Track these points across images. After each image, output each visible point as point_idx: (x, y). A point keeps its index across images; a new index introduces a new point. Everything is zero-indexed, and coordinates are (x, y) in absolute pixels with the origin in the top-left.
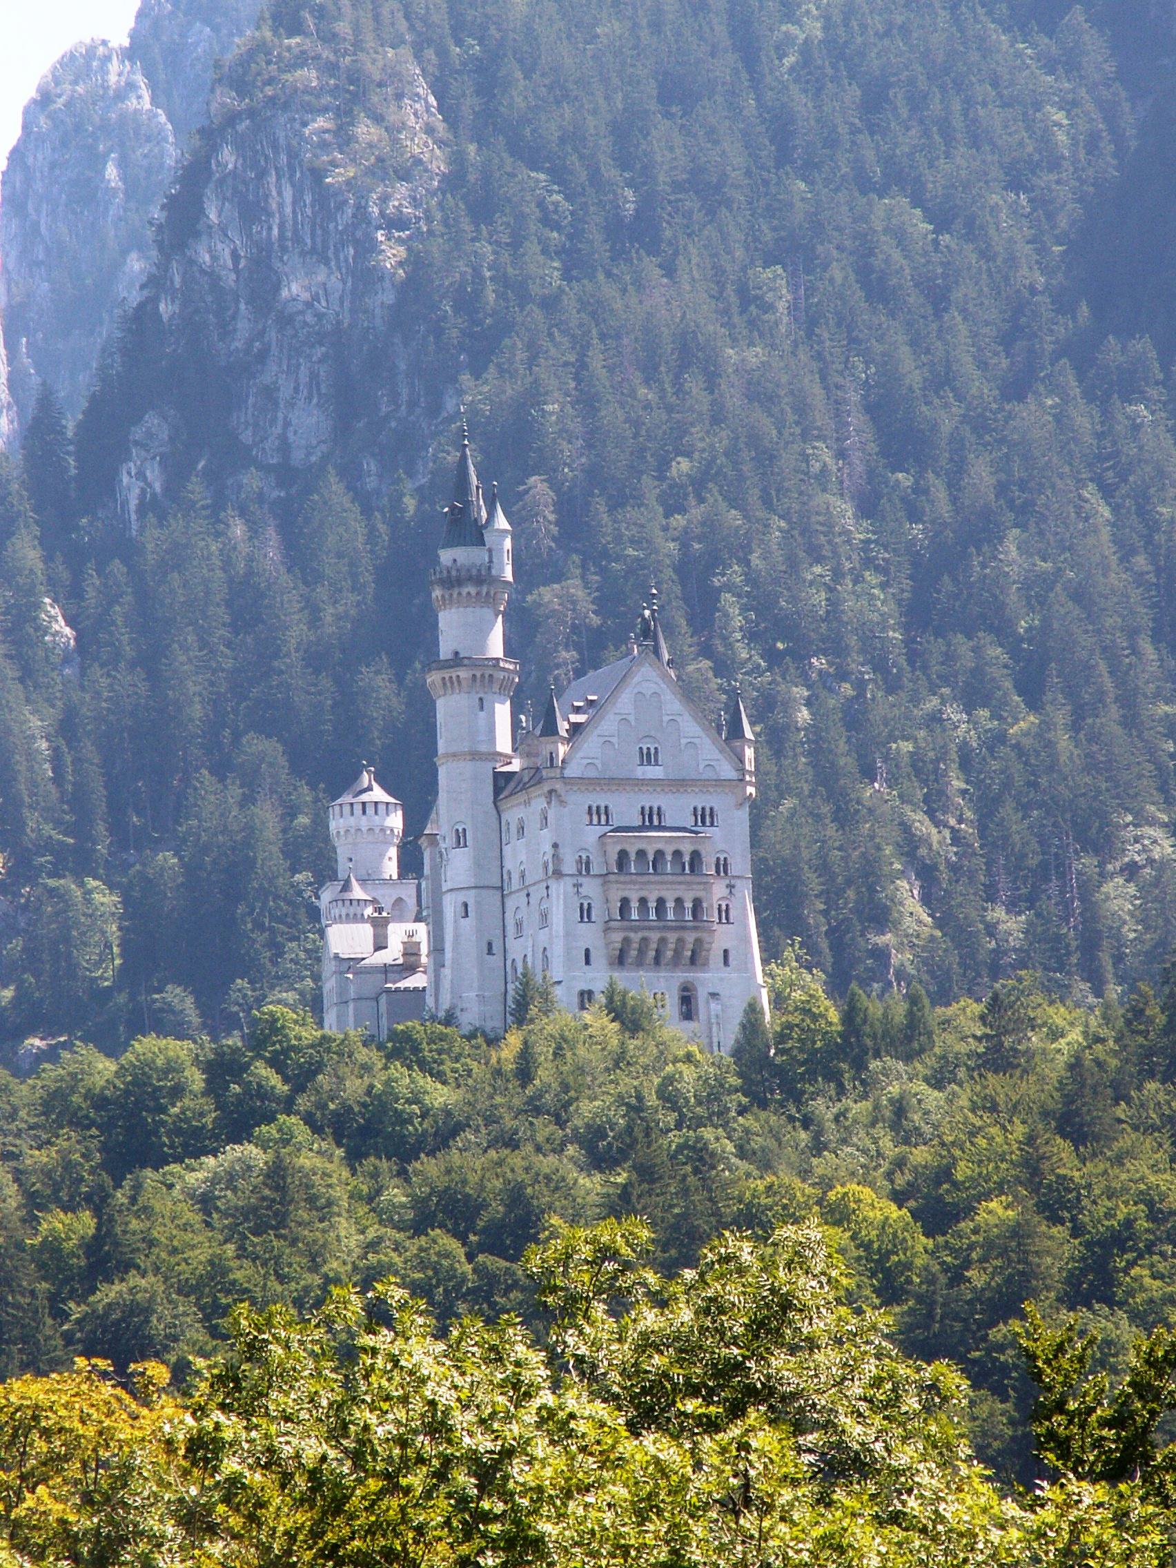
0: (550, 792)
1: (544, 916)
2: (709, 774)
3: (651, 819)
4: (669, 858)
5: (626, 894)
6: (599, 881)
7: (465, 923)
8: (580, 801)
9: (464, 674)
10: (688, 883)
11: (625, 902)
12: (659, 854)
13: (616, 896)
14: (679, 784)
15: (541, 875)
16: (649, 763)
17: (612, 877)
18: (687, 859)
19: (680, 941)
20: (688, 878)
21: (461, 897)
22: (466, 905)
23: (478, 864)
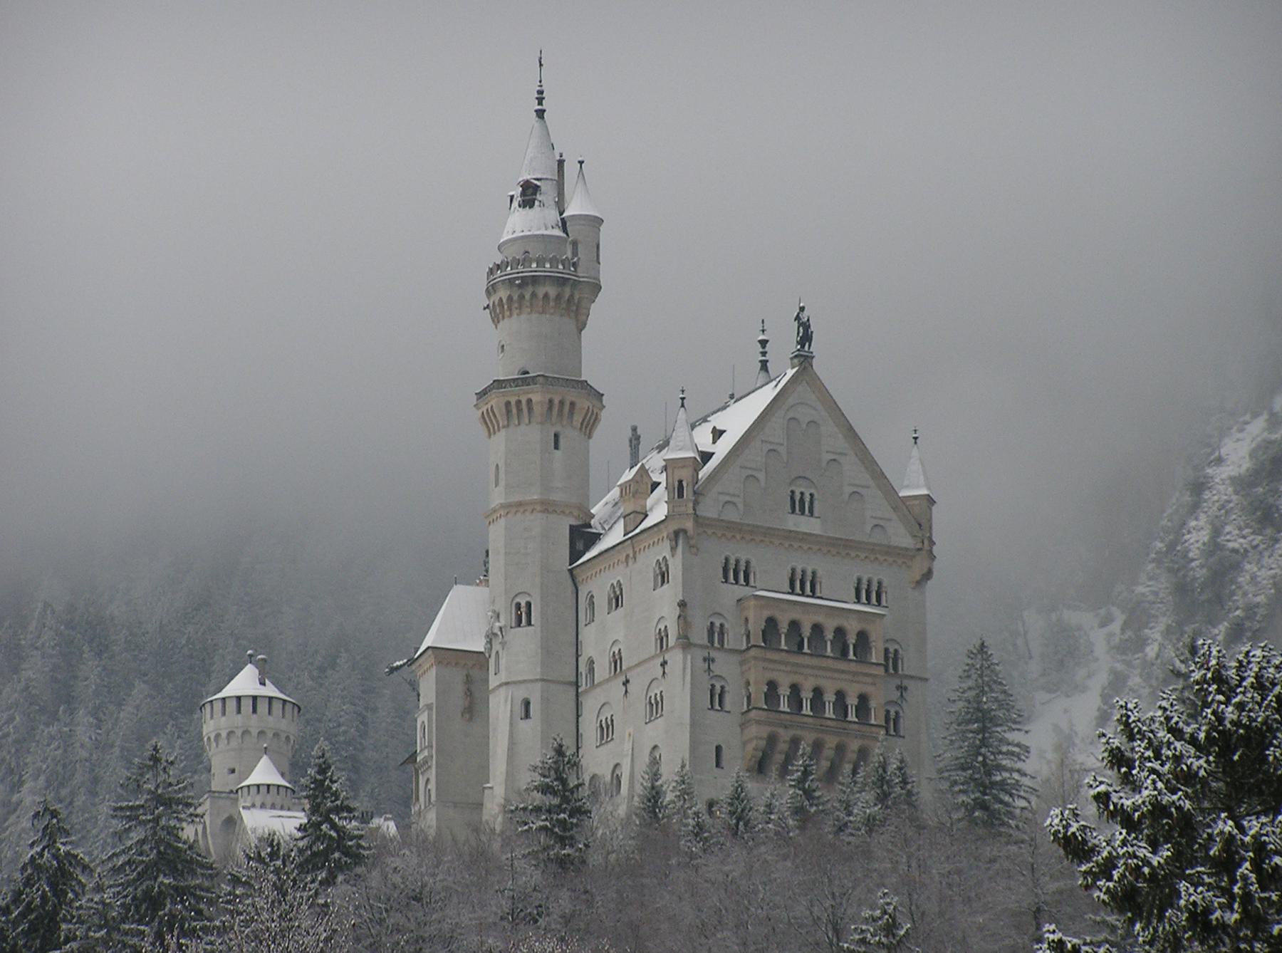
0: (677, 533)
1: (655, 706)
4: (829, 635)
6: (735, 658)
7: (524, 725)
10: (855, 674)
11: (772, 685)
13: (758, 677)
14: (840, 547)
15: (651, 647)
16: (803, 513)
17: (753, 652)
18: (852, 640)
20: (853, 667)
21: (521, 693)
22: (527, 704)
23: (547, 651)
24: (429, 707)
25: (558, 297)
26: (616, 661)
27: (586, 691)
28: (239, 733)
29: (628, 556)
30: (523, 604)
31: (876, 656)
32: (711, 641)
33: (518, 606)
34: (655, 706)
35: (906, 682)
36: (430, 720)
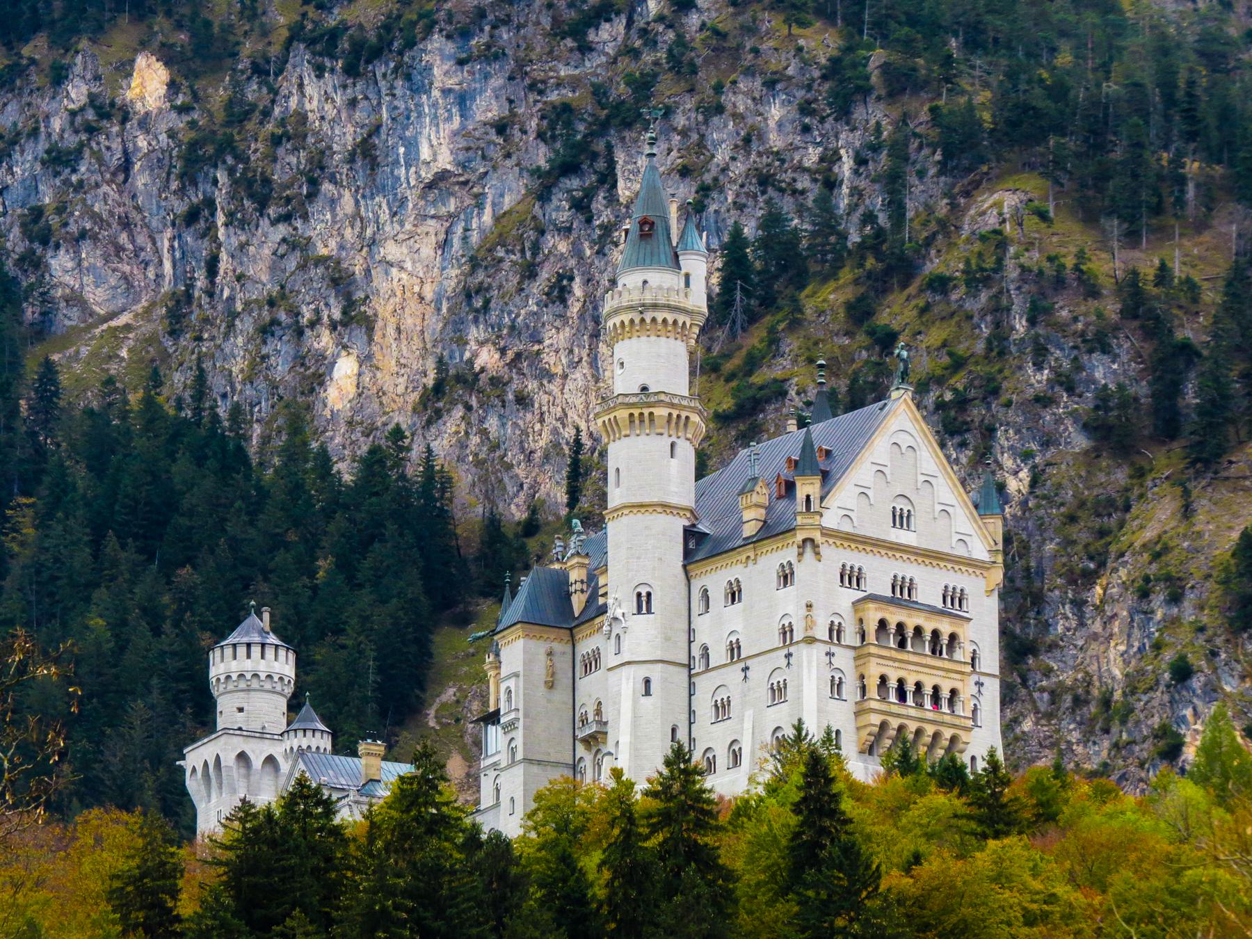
0: (804, 541)
1: (778, 692)
2: (960, 551)
3: (902, 593)
5: (885, 670)
6: (851, 654)
7: (645, 700)
8: (836, 557)
9: (661, 412)
11: (883, 679)
12: (918, 631)
13: (874, 671)
15: (778, 642)
18: (945, 640)
19: (936, 736)
22: (647, 682)
24: (516, 675)
25: (675, 322)
26: (734, 649)
27: (698, 674)
28: (248, 676)
29: (748, 557)
30: (644, 594)
31: (962, 655)
32: (831, 637)
33: (639, 595)
34: (778, 692)
35: (983, 679)
36: (517, 686)
